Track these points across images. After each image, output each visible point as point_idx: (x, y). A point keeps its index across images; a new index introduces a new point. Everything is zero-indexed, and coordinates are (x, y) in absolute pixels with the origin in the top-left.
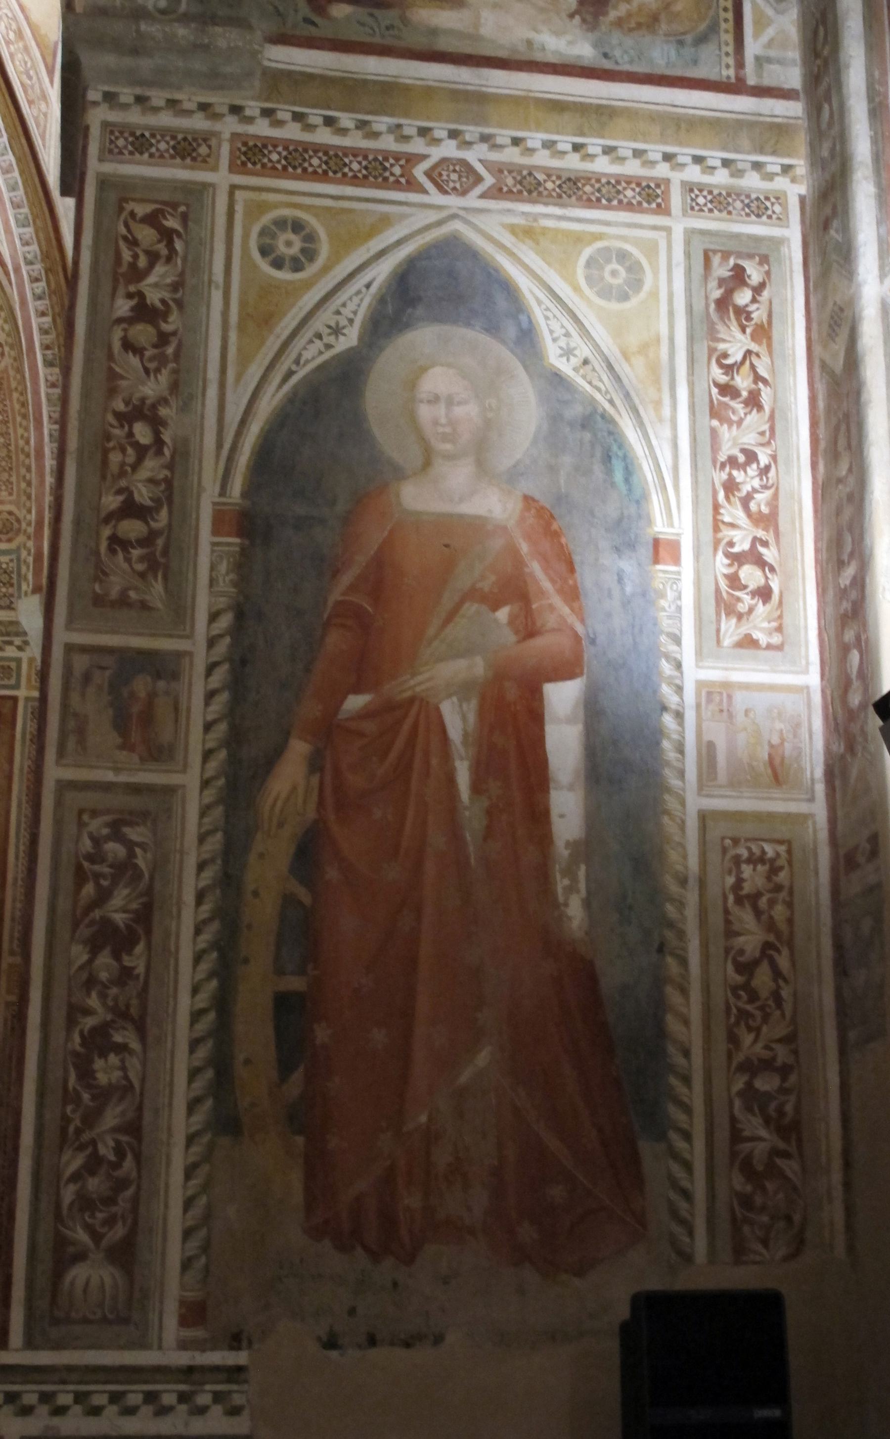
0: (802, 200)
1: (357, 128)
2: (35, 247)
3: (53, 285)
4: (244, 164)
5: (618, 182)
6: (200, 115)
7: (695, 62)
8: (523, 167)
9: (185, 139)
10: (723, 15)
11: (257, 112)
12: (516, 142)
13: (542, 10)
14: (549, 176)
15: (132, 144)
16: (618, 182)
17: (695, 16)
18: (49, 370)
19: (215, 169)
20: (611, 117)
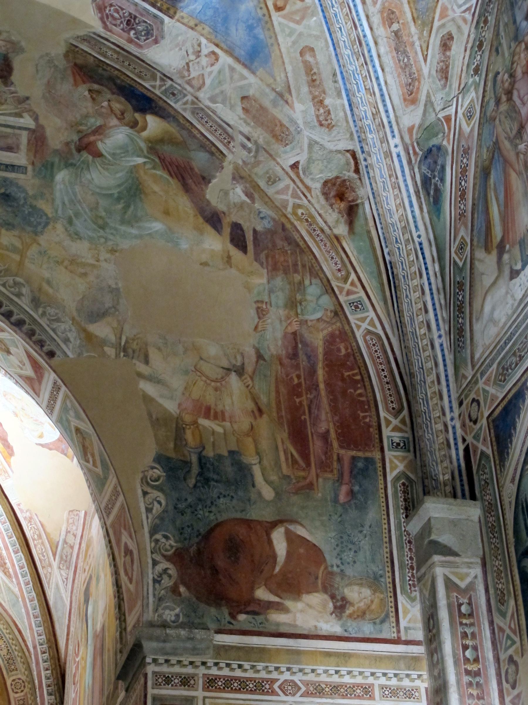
0: (426, 689)
1: (251, 669)
2: (44, 637)
3: (51, 654)
4: (208, 687)
5: (354, 687)
6: (190, 666)
7: (381, 631)
8: (317, 682)
9: (185, 678)
10: (391, 609)
11: (212, 664)
12: (313, 671)
13: (320, 612)
14: (327, 685)
15: (165, 680)
16: (354, 687)
17: (380, 611)
18: (50, 697)
19: (197, 690)
20: (349, 658)
